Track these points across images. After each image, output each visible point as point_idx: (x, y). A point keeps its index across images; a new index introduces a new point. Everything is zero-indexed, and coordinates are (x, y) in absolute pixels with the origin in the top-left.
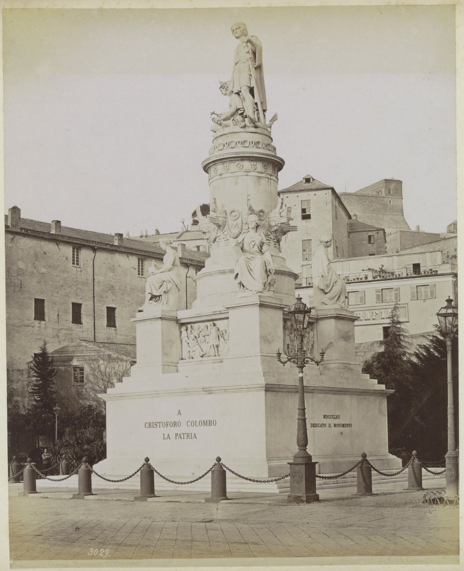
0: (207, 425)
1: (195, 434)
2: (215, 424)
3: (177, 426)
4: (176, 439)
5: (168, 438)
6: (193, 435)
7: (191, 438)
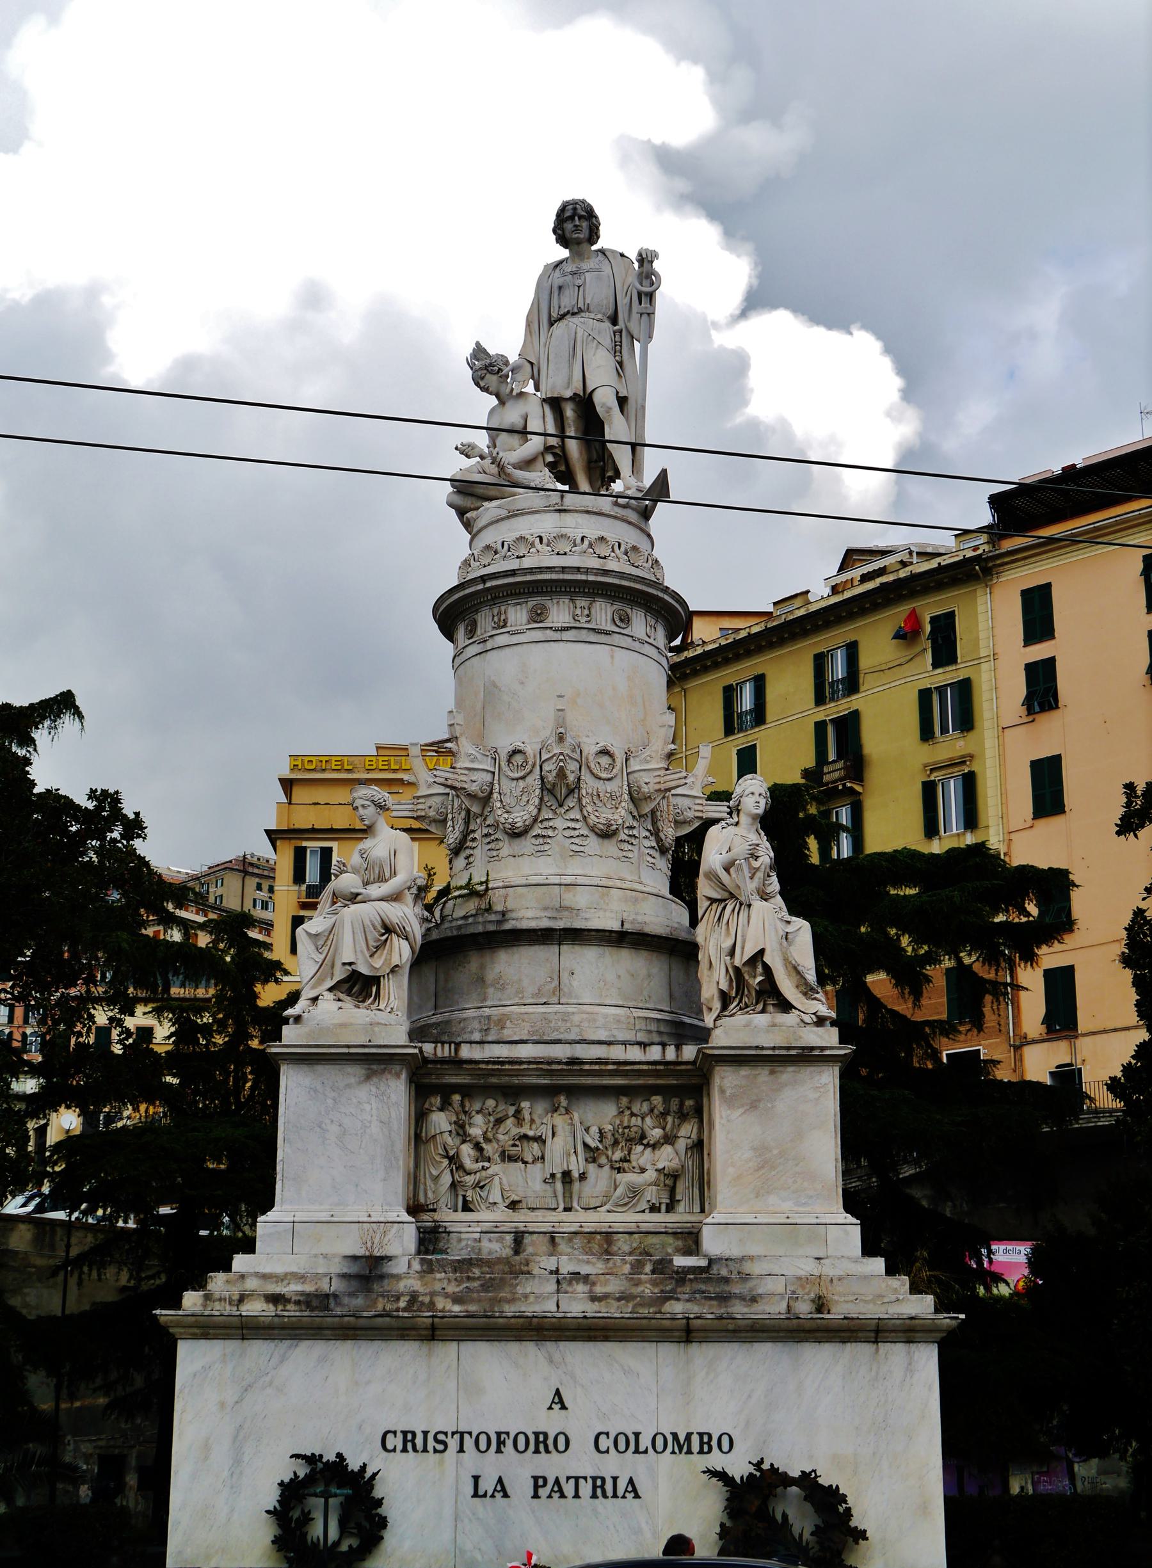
0: (689, 1452)
1: (631, 1481)
2: (726, 1447)
3: (551, 1447)
4: (536, 1496)
5: (499, 1495)
6: (622, 1485)
7: (615, 1496)
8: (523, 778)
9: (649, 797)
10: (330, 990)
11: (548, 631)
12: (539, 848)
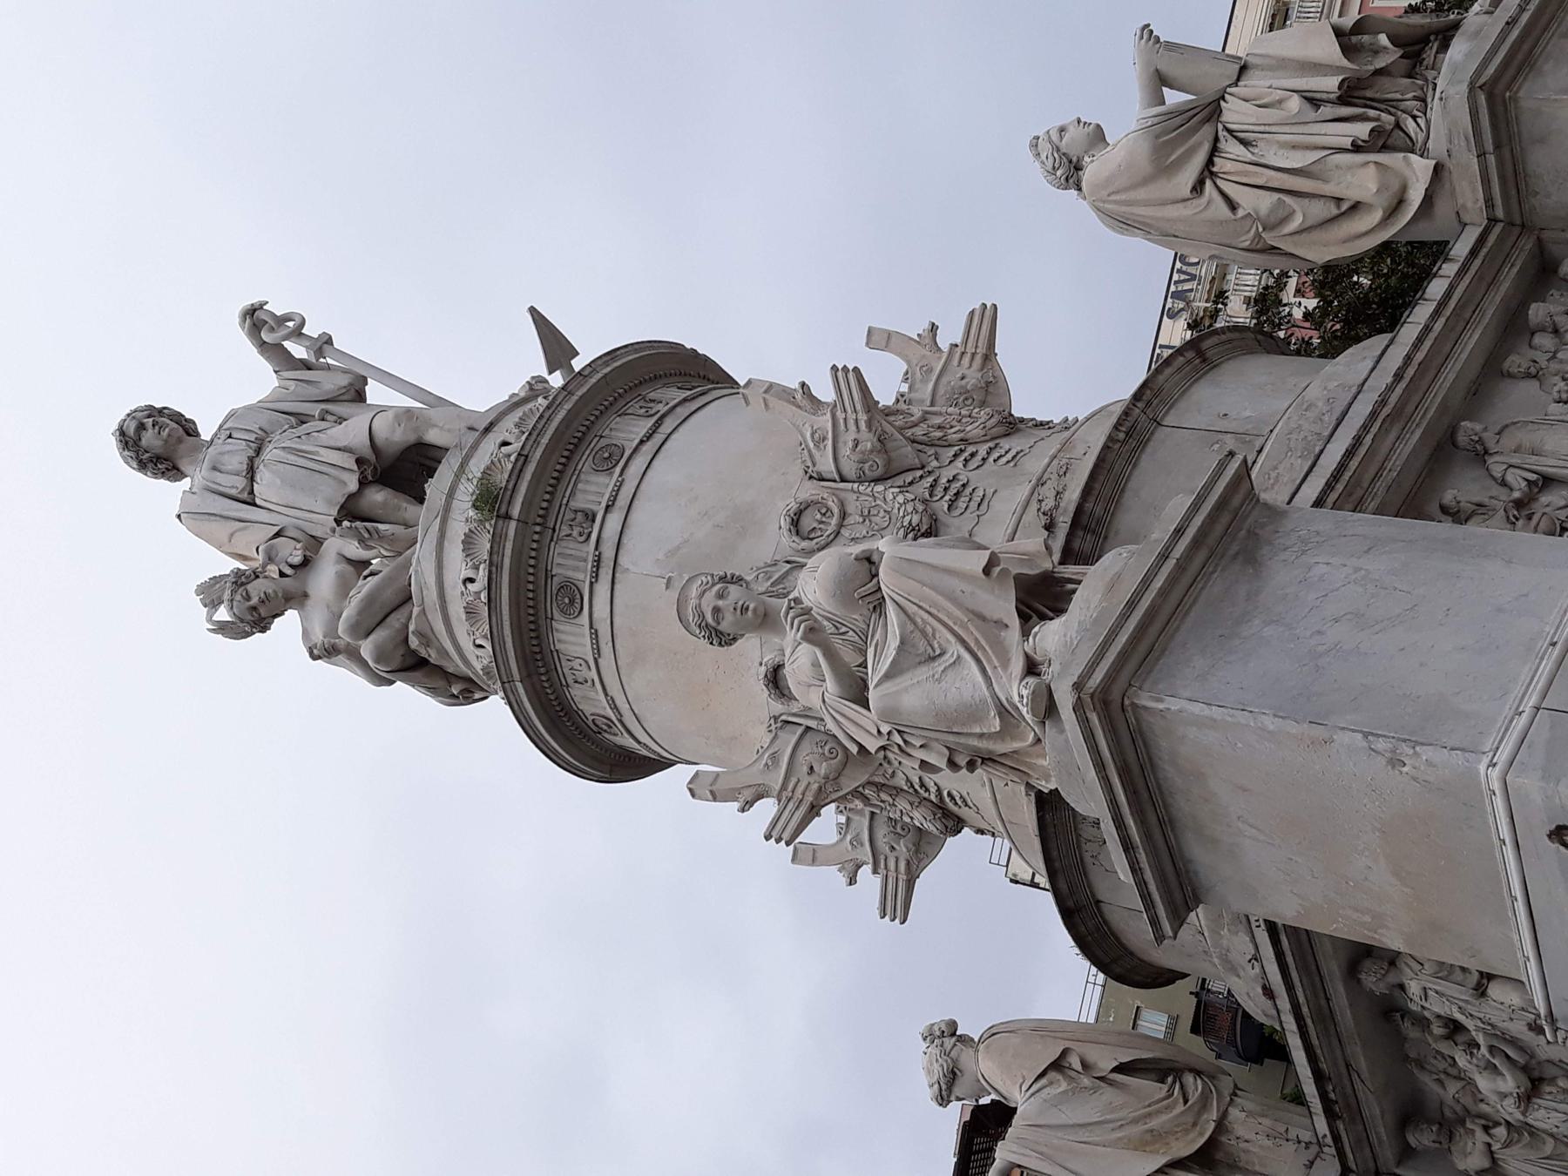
8: (844, 515)
9: (988, 383)
10: (1026, 634)
11: (645, 448)
12: (974, 505)
